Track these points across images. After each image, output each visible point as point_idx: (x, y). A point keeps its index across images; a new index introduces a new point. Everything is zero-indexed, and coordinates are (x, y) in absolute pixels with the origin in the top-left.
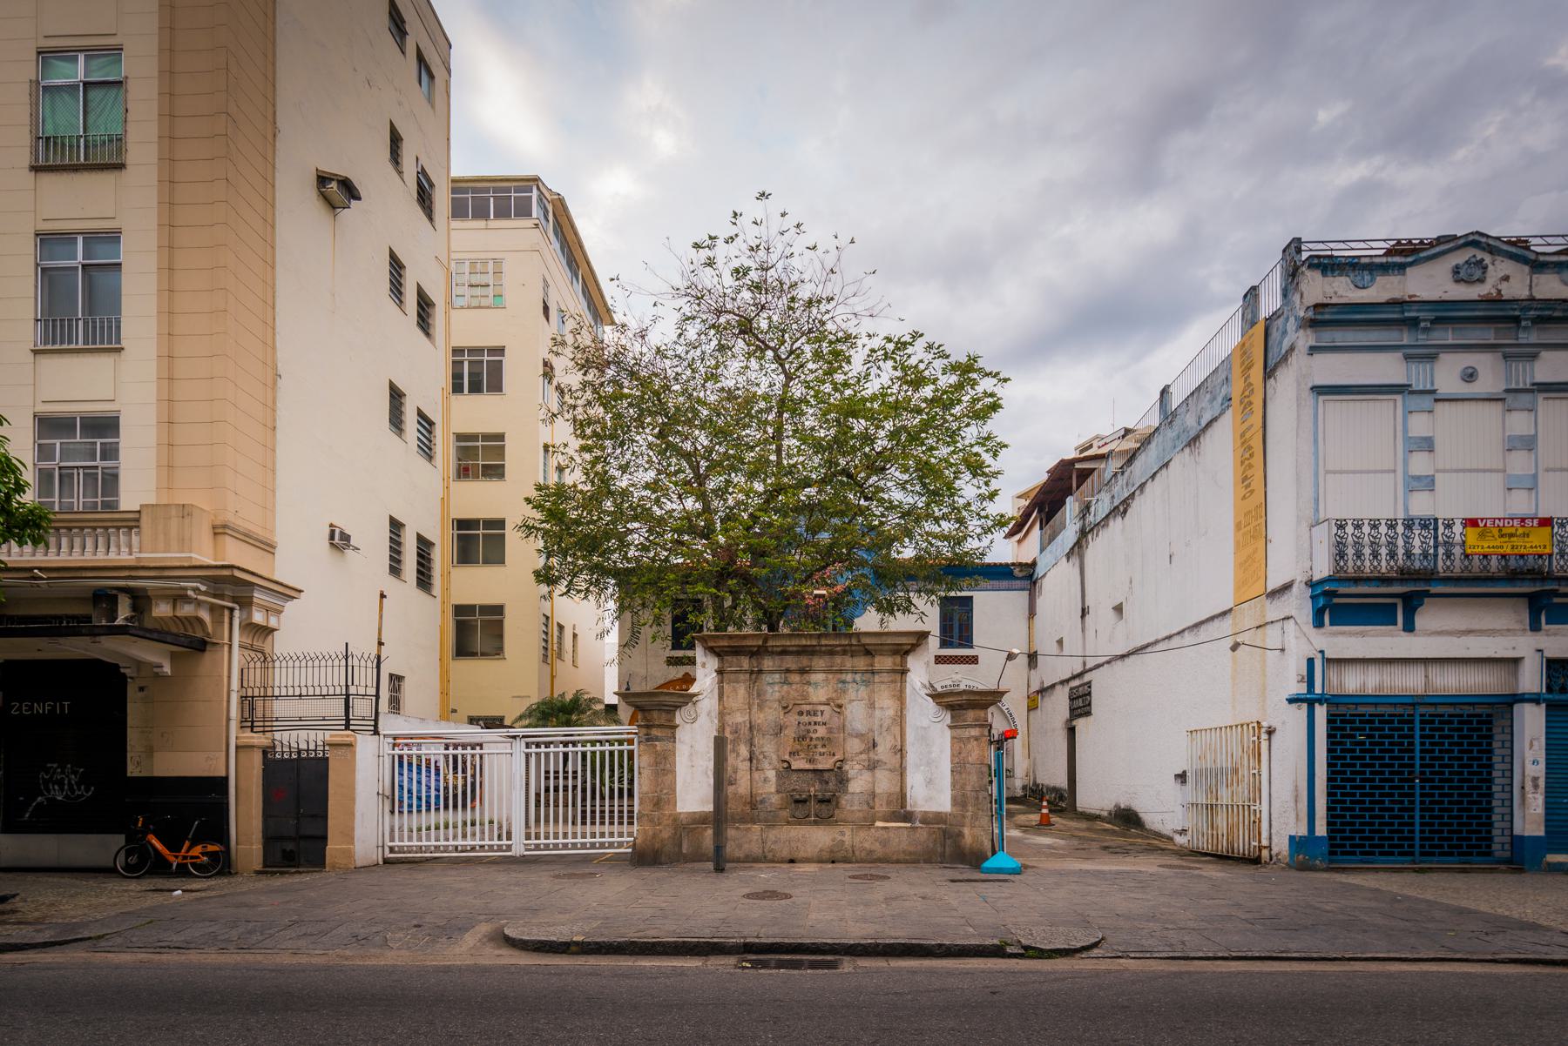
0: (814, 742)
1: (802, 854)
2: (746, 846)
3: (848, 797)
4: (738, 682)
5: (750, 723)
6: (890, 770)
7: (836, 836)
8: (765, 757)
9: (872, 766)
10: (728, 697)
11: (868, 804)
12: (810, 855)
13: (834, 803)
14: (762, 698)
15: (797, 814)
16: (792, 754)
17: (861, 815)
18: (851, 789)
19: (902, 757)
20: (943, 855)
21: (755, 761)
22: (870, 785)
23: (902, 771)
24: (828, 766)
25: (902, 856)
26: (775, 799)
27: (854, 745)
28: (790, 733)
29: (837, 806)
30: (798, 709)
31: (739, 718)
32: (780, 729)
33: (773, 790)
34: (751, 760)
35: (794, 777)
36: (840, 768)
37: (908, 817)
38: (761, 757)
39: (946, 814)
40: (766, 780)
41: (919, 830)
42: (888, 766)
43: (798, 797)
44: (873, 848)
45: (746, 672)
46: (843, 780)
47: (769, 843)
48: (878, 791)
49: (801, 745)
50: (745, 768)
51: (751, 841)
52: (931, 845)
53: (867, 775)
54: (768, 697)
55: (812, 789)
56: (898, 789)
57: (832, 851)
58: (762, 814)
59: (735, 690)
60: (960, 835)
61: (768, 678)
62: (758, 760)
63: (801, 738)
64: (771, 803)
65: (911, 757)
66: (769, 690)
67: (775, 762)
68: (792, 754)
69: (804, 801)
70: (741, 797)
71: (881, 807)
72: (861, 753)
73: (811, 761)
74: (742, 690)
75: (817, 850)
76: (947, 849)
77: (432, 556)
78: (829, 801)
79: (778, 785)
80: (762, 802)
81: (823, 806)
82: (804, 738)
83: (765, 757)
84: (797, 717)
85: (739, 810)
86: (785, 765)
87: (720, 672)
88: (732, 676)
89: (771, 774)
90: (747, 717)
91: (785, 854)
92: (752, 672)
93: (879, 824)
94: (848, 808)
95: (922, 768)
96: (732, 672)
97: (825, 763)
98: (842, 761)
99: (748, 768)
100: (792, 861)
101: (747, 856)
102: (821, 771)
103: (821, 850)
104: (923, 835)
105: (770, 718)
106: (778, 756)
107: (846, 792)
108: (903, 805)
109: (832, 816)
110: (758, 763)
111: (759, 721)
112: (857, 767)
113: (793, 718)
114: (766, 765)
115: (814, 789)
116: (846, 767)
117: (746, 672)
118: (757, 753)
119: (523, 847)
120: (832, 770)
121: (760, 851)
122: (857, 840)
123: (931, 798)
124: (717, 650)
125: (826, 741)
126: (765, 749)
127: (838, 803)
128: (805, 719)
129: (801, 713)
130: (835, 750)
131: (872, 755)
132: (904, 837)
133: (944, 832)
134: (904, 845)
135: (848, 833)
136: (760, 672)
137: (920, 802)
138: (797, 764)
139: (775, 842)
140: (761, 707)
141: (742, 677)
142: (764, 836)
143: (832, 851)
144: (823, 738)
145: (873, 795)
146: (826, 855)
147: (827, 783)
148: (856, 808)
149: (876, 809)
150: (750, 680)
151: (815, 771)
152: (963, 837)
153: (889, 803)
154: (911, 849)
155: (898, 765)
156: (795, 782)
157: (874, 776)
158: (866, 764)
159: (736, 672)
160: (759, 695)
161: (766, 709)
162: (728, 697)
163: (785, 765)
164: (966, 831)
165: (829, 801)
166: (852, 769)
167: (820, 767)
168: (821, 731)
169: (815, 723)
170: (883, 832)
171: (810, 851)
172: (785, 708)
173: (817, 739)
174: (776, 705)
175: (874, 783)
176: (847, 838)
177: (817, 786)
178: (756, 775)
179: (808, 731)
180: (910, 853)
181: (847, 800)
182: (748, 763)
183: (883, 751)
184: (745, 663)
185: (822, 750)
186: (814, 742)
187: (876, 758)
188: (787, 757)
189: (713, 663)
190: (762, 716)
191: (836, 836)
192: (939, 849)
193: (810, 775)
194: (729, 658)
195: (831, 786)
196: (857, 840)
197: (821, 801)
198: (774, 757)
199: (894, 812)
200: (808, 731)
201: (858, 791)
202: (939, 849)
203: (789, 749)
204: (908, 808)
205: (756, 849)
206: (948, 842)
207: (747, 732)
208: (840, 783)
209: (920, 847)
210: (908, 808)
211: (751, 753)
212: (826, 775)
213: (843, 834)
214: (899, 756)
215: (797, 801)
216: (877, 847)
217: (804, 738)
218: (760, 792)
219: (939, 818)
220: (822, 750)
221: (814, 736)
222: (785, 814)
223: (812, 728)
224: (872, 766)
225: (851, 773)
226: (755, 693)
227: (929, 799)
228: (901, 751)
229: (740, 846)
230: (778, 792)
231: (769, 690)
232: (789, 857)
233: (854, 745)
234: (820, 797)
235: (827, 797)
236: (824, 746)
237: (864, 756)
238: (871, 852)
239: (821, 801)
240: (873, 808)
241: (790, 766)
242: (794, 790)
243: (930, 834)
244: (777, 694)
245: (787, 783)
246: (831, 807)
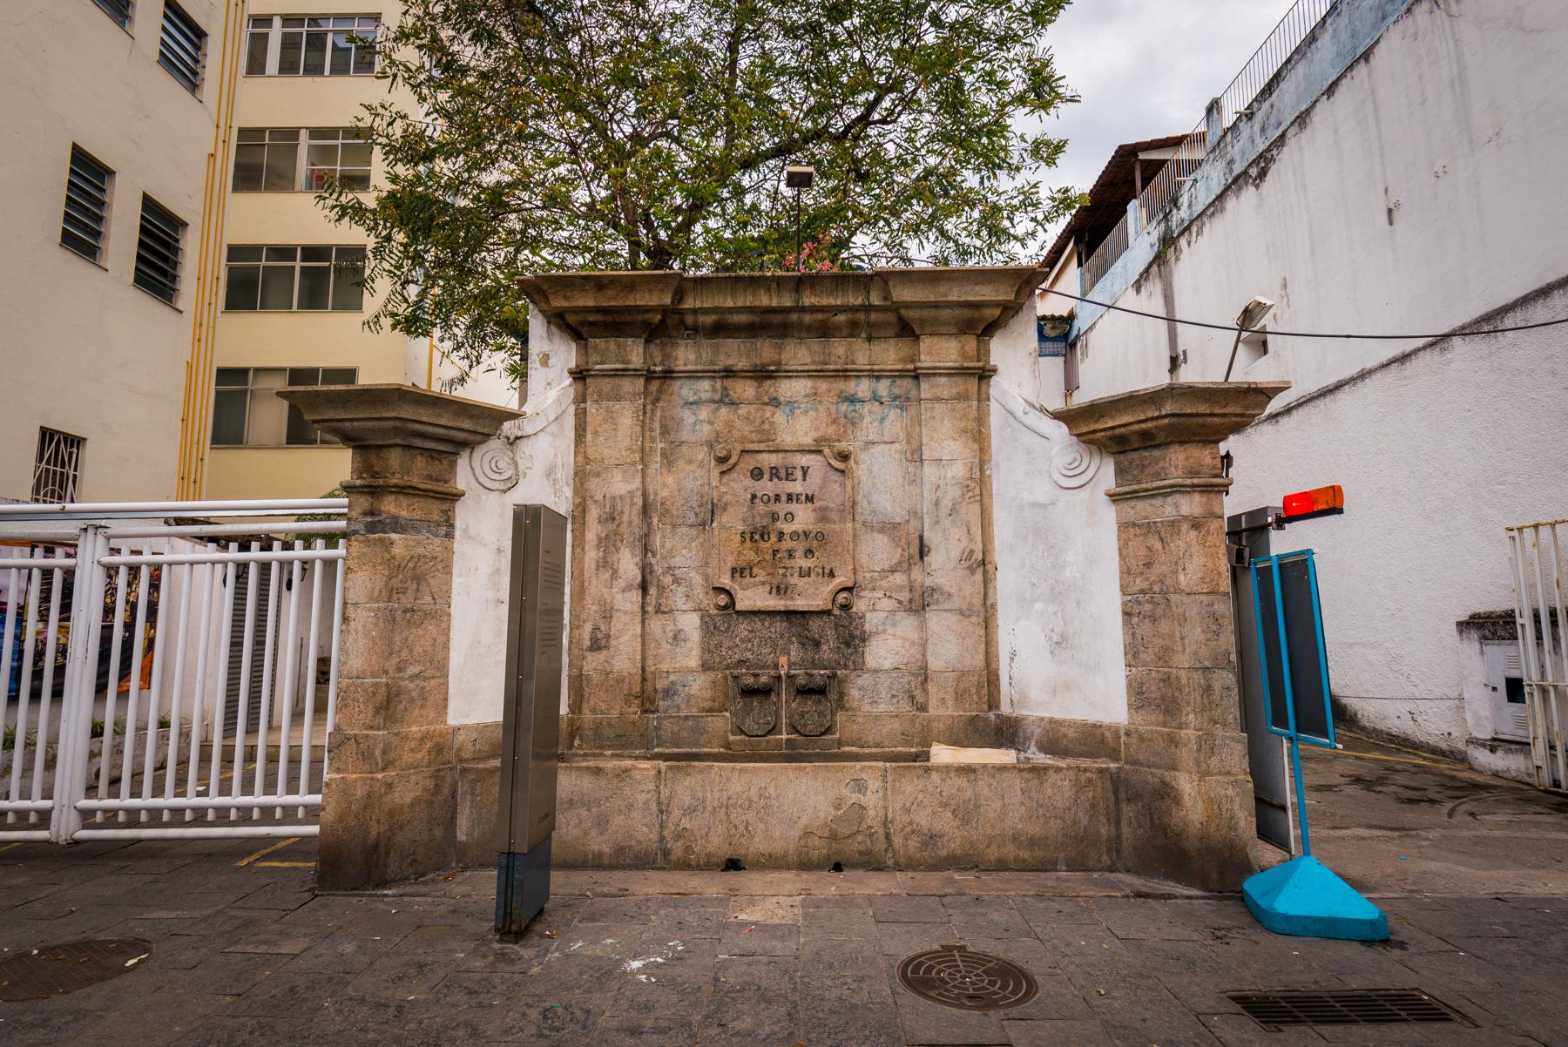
0: (787, 544)
1: (758, 845)
2: (618, 821)
3: (864, 680)
4: (617, 398)
5: (645, 496)
6: (961, 613)
7: (846, 792)
8: (676, 581)
9: (919, 603)
10: (596, 433)
11: (912, 698)
12: (777, 847)
13: (833, 696)
14: (672, 437)
15: (749, 724)
16: (738, 572)
17: (896, 725)
18: (870, 662)
19: (987, 581)
20: (1115, 844)
21: (653, 591)
22: (916, 650)
23: (986, 615)
24: (817, 603)
25: (1010, 851)
26: (698, 686)
27: (877, 552)
28: (733, 521)
29: (841, 703)
30: (750, 463)
31: (621, 485)
32: (712, 510)
33: (693, 662)
34: (644, 587)
35: (743, 629)
36: (846, 607)
37: (1006, 733)
38: (668, 580)
39: (1115, 731)
40: (677, 638)
41: (1052, 776)
42: (956, 603)
43: (750, 680)
44: (938, 827)
45: (636, 373)
46: (853, 639)
47: (676, 813)
48: (935, 664)
49: (757, 551)
50: (628, 607)
51: (630, 807)
52: (1085, 821)
53: (906, 626)
54: (685, 434)
55: (783, 660)
56: (979, 660)
57: (833, 836)
58: (666, 724)
59: (611, 417)
60: (1167, 793)
61: (685, 390)
62: (661, 589)
63: (757, 535)
64: (690, 697)
65: (1007, 582)
66: (688, 417)
67: (699, 591)
68: (738, 572)
69: (764, 692)
70: (620, 681)
71: (943, 708)
72: (893, 571)
73: (780, 590)
74: (627, 417)
75: (796, 833)
76: (1126, 831)
77: (182, 245)
78: (821, 691)
79: (706, 650)
80: (669, 692)
81: (810, 704)
82: (764, 534)
83: (676, 581)
84: (749, 482)
85: (615, 714)
86: (722, 600)
87: (580, 375)
88: (606, 385)
89: (690, 623)
90: (636, 483)
91: (716, 844)
92: (649, 376)
93: (942, 754)
94: (866, 708)
95: (1038, 606)
96: (606, 374)
97: (812, 596)
98: (849, 589)
99: (637, 607)
100: (733, 865)
101: (620, 851)
102: (803, 613)
103: (807, 833)
104: (1060, 790)
105: (689, 484)
106: (706, 577)
107: (860, 667)
108: (993, 704)
109: (828, 730)
110: (659, 596)
111: (664, 493)
112: (886, 604)
113: (739, 486)
114: (678, 600)
115: (788, 660)
116: (860, 606)
117: (636, 373)
118: (659, 570)
119: (74, 818)
120: (828, 613)
121: (654, 836)
122: (895, 806)
123: (1067, 686)
124: (571, 319)
125: (815, 541)
126: (678, 561)
127: (842, 695)
128: (767, 486)
129: (757, 474)
130: (835, 563)
131: (917, 575)
132: (1015, 797)
133: (1116, 781)
134: (1015, 819)
135: (874, 784)
136: (669, 375)
137: (1036, 694)
138: (753, 597)
139: (690, 811)
140: (668, 459)
141: (628, 386)
142: (665, 793)
143: (833, 836)
144: (806, 534)
145: (923, 675)
146: (818, 847)
147: (817, 644)
148: (882, 708)
149: (932, 712)
150: (646, 393)
151: (788, 614)
152: (1177, 799)
153: (959, 696)
154: (1035, 829)
155: (977, 601)
156: (745, 642)
157: (923, 627)
158: (905, 596)
159: (615, 374)
160: (665, 430)
161: (681, 463)
162: (596, 433)
163: (722, 600)
164: (1186, 784)
165: (821, 691)
166: (874, 610)
167: (800, 604)
168: (804, 518)
169: (790, 498)
170: (961, 781)
171: (776, 835)
172: (721, 460)
173: (795, 535)
174: (702, 454)
175: (924, 646)
176: (871, 800)
177: (795, 652)
178: (656, 625)
179: (774, 517)
180: (1032, 842)
181: (861, 688)
182: (636, 595)
183: (943, 567)
184: (636, 353)
185: (805, 563)
186: (787, 544)
187: (928, 582)
188: (726, 581)
189: (565, 354)
190: (670, 480)
191: (846, 792)
192: (1105, 830)
193: (780, 625)
194: (600, 342)
195: (827, 652)
196: (895, 806)
197: (805, 692)
198: (697, 579)
199: (973, 719)
200: (774, 517)
201: (887, 665)
202: (1105, 830)
203: (730, 562)
204: (1005, 709)
205: (641, 830)
206: (1129, 811)
207: (636, 519)
208: (848, 645)
209: (1054, 826)
210: (1005, 709)
211: (646, 570)
212: (815, 625)
213: (860, 786)
214: (979, 577)
215: (748, 692)
216: (946, 823)
217: (764, 534)
218: (664, 667)
219: (1093, 740)
220: (805, 563)
221: (787, 528)
222: (720, 723)
223: (783, 508)
224: (919, 603)
225: (872, 621)
226: (657, 425)
227: (1062, 688)
228: (982, 565)
229: (602, 822)
230: (706, 667)
231: (688, 417)
232: (725, 852)
233: (877, 552)
234: (801, 681)
235: (819, 681)
236: (809, 552)
237: (899, 578)
238: (931, 838)
239: (805, 692)
240: (923, 708)
241: (733, 603)
242: (741, 663)
243: (1079, 788)
244: (706, 428)
245: (727, 644)
246: (826, 706)
